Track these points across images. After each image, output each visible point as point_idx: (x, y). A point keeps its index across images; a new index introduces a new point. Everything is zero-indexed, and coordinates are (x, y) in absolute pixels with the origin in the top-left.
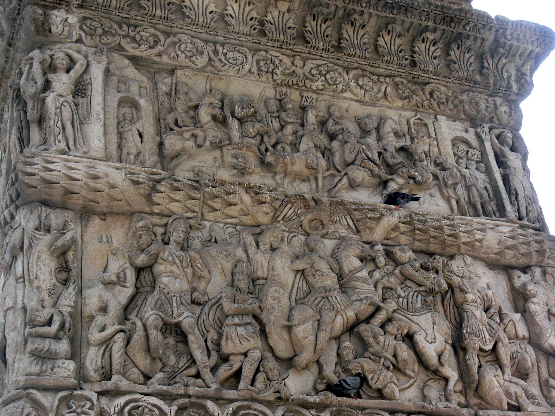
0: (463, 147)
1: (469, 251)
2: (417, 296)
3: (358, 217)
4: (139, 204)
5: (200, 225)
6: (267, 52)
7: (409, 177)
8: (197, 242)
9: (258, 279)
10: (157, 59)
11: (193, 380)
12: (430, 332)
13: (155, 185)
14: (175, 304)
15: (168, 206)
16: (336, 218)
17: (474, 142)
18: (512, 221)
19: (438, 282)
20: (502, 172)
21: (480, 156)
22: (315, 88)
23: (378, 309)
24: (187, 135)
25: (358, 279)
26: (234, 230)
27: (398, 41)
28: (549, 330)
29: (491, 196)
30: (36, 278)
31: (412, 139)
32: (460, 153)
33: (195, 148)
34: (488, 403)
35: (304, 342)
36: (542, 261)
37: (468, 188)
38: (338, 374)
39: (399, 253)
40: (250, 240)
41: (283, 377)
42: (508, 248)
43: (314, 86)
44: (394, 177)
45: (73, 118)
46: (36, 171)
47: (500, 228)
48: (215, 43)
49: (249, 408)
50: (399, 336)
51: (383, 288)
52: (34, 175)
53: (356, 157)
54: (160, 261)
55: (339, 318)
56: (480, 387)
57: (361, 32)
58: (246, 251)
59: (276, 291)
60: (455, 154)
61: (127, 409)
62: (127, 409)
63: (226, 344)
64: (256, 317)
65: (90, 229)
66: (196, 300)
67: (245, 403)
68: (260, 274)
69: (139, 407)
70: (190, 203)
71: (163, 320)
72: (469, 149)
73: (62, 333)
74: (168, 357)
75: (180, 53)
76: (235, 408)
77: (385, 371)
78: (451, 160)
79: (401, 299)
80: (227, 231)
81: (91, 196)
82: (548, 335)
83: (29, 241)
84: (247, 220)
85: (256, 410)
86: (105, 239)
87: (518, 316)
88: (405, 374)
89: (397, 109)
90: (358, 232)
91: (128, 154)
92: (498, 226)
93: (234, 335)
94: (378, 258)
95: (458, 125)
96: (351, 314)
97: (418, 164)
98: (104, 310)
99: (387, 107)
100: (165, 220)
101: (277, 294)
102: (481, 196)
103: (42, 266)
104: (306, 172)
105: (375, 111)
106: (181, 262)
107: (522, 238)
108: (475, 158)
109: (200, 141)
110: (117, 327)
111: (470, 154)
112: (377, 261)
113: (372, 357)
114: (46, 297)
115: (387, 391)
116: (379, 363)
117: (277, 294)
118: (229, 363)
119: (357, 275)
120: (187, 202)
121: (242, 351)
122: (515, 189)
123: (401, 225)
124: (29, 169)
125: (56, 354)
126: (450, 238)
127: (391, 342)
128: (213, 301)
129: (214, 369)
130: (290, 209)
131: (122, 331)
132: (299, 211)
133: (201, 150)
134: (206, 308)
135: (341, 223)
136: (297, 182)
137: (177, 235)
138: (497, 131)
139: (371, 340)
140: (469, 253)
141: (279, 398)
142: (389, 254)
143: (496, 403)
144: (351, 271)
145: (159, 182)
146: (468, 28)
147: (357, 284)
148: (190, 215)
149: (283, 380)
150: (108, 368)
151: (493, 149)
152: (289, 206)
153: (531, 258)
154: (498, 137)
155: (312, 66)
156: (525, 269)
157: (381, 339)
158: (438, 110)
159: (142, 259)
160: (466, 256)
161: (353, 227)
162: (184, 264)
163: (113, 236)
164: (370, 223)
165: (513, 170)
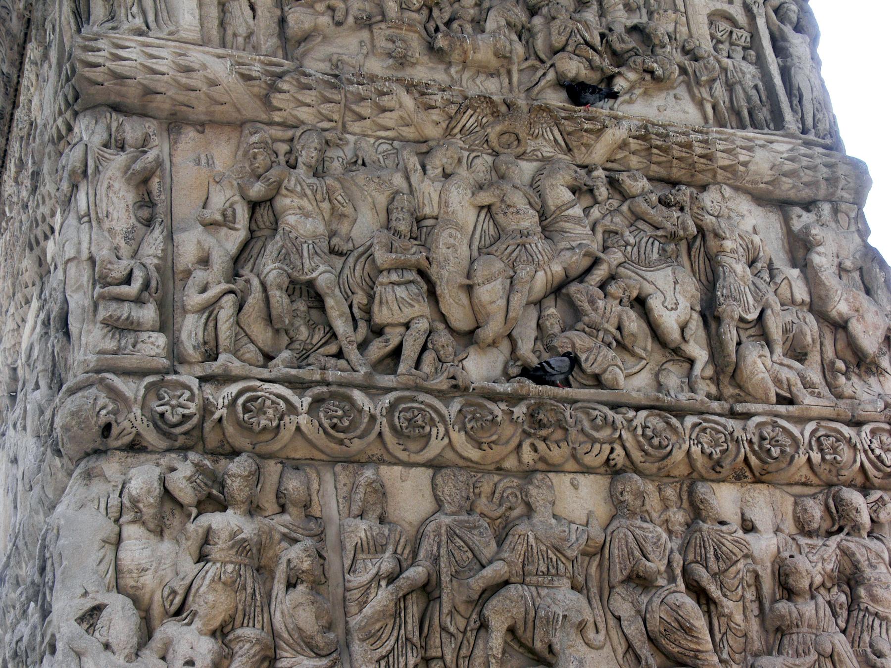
0: (724, 25)
1: (729, 179)
2: (653, 244)
3: (569, 129)
4: (252, 109)
5: (340, 139)
7: (645, 71)
8: (336, 164)
9: (425, 218)
11: (333, 361)
12: (670, 294)
13: (275, 82)
14: (305, 254)
15: (295, 112)
16: (537, 131)
17: (741, 18)
18: (792, 136)
19: (683, 223)
20: (781, 64)
21: (749, 39)
23: (596, 262)
25: (568, 219)
26: (390, 147)
28: (839, 292)
29: (764, 98)
30: (107, 217)
31: (650, 14)
32: (720, 34)
33: (332, 27)
34: (749, 394)
35: (492, 308)
36: (833, 194)
37: (730, 88)
38: (538, 353)
39: (628, 181)
40: (413, 162)
41: (460, 357)
42: (785, 175)
44: (623, 70)
46: (101, 60)
47: (775, 146)
49: (413, 400)
50: (625, 300)
51: (604, 232)
53: (567, 40)
54: (284, 191)
55: (541, 274)
56: (738, 372)
58: (408, 178)
59: (451, 236)
60: (712, 37)
61: (241, 401)
62: (241, 401)
63: (380, 311)
64: (422, 273)
65: (181, 146)
66: (336, 248)
67: (407, 393)
68: (427, 211)
69: (258, 398)
70: (325, 108)
71: (289, 276)
72: (734, 29)
73: (146, 294)
74: (297, 329)
76: (392, 399)
77: (605, 350)
78: (707, 46)
79: (629, 248)
80: (380, 149)
81: (182, 97)
82: (837, 299)
83: (95, 162)
84: (409, 133)
85: (422, 403)
86: (203, 161)
87: (795, 272)
88: (633, 354)
90: (570, 150)
91: (235, 35)
92: (771, 142)
93: (391, 297)
94: (598, 189)
96: (557, 269)
97: (659, 51)
98: (205, 261)
100: (289, 133)
101: (452, 241)
102: (749, 99)
103: (115, 200)
104: (494, 63)
106: (315, 193)
107: (805, 162)
108: (742, 42)
109: (339, 16)
110: (224, 286)
111: (734, 36)
112: (596, 192)
113: (587, 329)
114: (122, 244)
115: (607, 377)
116: (596, 338)
117: (452, 241)
118: (384, 337)
119: (566, 213)
120: (322, 106)
121: (402, 321)
122: (799, 89)
123: (631, 140)
124: (91, 57)
125: (139, 324)
126: (702, 160)
127: (614, 308)
128: (361, 249)
129: (363, 346)
130: (471, 116)
131: (231, 292)
132: (485, 120)
133: (341, 29)
134: (351, 260)
135: (545, 138)
136: (482, 77)
137: (307, 154)
139: (586, 306)
140: (728, 182)
141: (455, 387)
142: (613, 183)
143: (760, 394)
144: (558, 208)
145: (280, 76)
147: (567, 225)
148: (326, 125)
149: (461, 361)
150: (212, 343)
151: (769, 28)
152: (470, 112)
153: (817, 189)
154: (776, 11)
156: (808, 205)
157: (601, 304)
159: (257, 190)
160: (724, 186)
161: (563, 144)
162: (319, 197)
163: (216, 155)
164: (587, 138)
165: (796, 60)
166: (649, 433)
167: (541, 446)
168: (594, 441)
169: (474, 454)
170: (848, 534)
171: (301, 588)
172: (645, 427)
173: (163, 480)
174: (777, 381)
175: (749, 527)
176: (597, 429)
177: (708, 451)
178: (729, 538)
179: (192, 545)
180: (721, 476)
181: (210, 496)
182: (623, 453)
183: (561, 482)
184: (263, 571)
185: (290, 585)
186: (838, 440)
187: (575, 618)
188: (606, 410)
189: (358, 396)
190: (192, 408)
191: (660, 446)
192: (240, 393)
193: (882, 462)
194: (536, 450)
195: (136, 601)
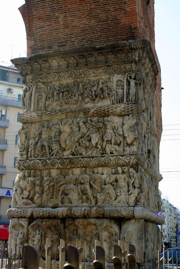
0: (119, 82)
6: (71, 71)
10: (47, 81)
12: (95, 138)
22: (82, 77)
24: (50, 100)
27: (103, 57)
37: (117, 95)
40: (60, 123)
42: (123, 111)
43: (82, 76)
45: (29, 104)
47: (121, 106)
48: (59, 72)
49: (54, 160)
52: (21, 119)
57: (93, 58)
58: (59, 126)
65: (32, 126)
67: (54, 159)
68: (61, 130)
70: (49, 117)
75: (51, 78)
81: (31, 120)
84: (61, 118)
89: (104, 75)
95: (120, 76)
98: (32, 144)
99: (101, 76)
105: (98, 78)
136: (74, 105)
138: (129, 75)
146: (120, 48)
148: (49, 119)
152: (69, 113)
155: (82, 71)
156: (128, 115)
158: (114, 73)
164: (87, 113)
165: (131, 86)
166: (87, 161)
167: (71, 165)
168: (78, 164)
169: (62, 167)
170: (118, 174)
171: (38, 186)
172: (86, 161)
173: (24, 174)
174: (111, 150)
175: (103, 174)
176: (79, 162)
177: (96, 163)
178: (97, 176)
179: (27, 181)
180: (99, 166)
181: (29, 175)
182: (82, 165)
183: (74, 169)
184: (35, 184)
185: (37, 186)
186: (119, 159)
187: (72, 189)
188: (81, 159)
189: (47, 161)
190: (28, 165)
191: (88, 163)
192: (33, 162)
193: (126, 162)
194: (70, 166)
195: (21, 188)
